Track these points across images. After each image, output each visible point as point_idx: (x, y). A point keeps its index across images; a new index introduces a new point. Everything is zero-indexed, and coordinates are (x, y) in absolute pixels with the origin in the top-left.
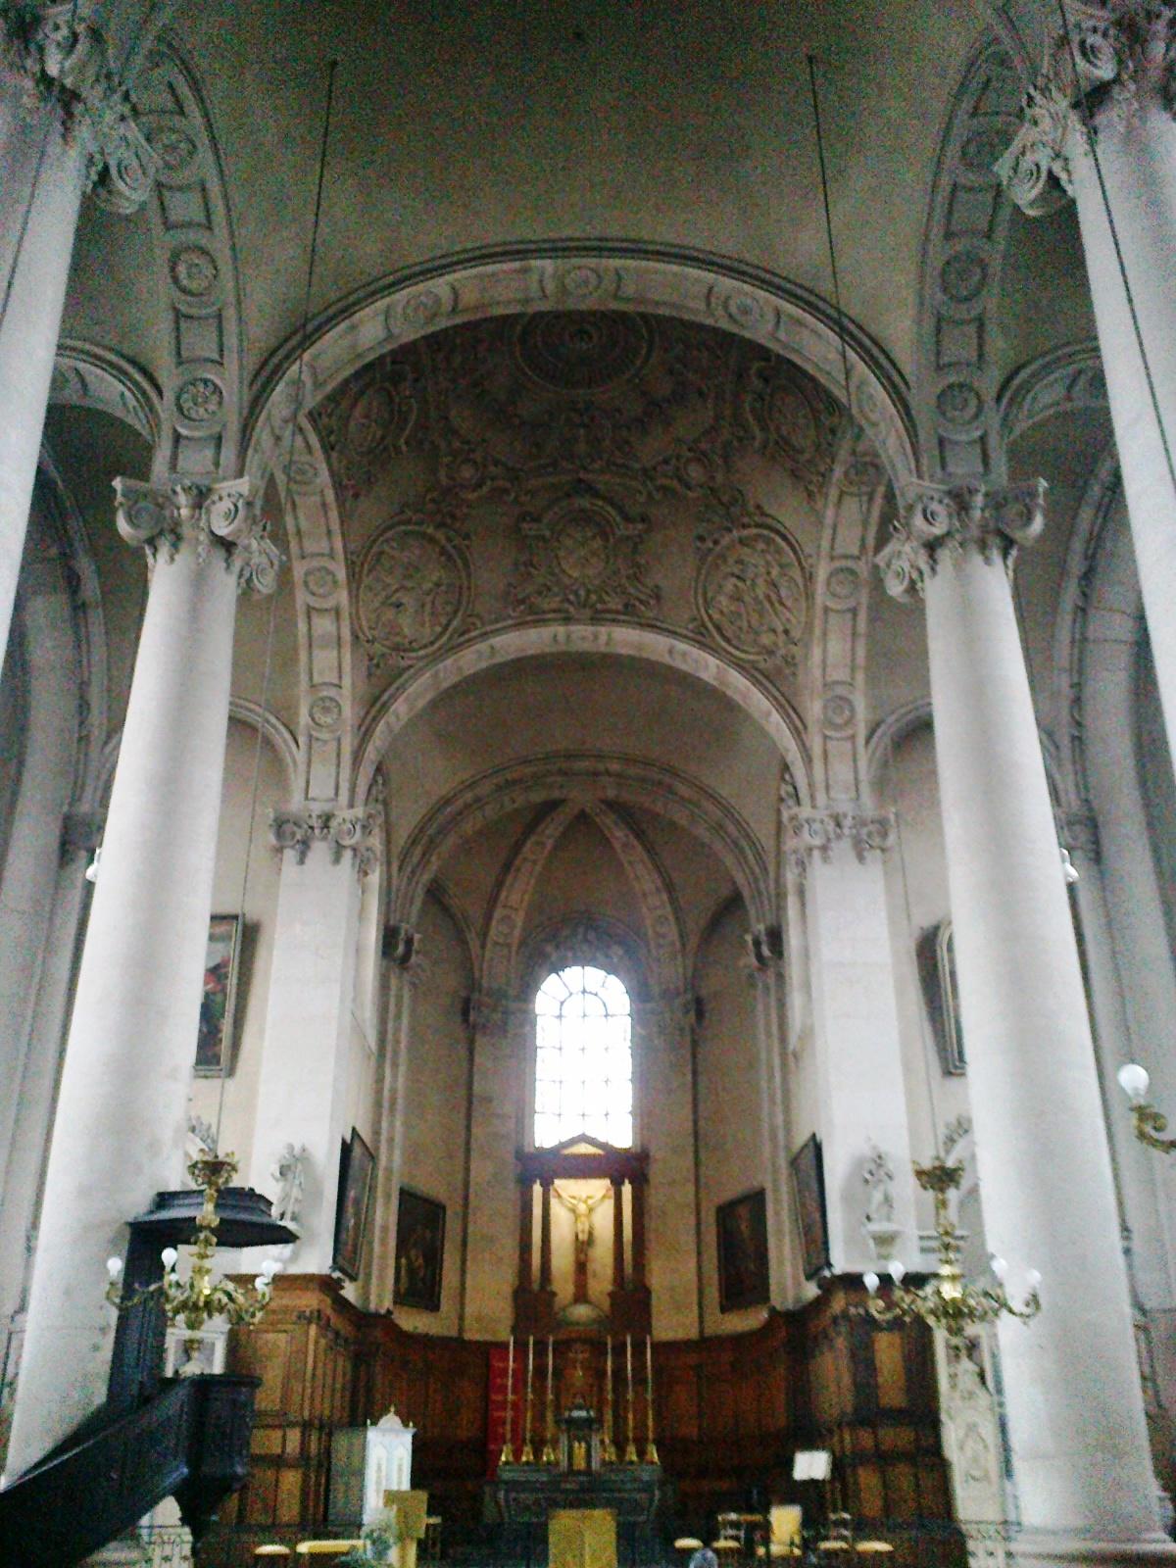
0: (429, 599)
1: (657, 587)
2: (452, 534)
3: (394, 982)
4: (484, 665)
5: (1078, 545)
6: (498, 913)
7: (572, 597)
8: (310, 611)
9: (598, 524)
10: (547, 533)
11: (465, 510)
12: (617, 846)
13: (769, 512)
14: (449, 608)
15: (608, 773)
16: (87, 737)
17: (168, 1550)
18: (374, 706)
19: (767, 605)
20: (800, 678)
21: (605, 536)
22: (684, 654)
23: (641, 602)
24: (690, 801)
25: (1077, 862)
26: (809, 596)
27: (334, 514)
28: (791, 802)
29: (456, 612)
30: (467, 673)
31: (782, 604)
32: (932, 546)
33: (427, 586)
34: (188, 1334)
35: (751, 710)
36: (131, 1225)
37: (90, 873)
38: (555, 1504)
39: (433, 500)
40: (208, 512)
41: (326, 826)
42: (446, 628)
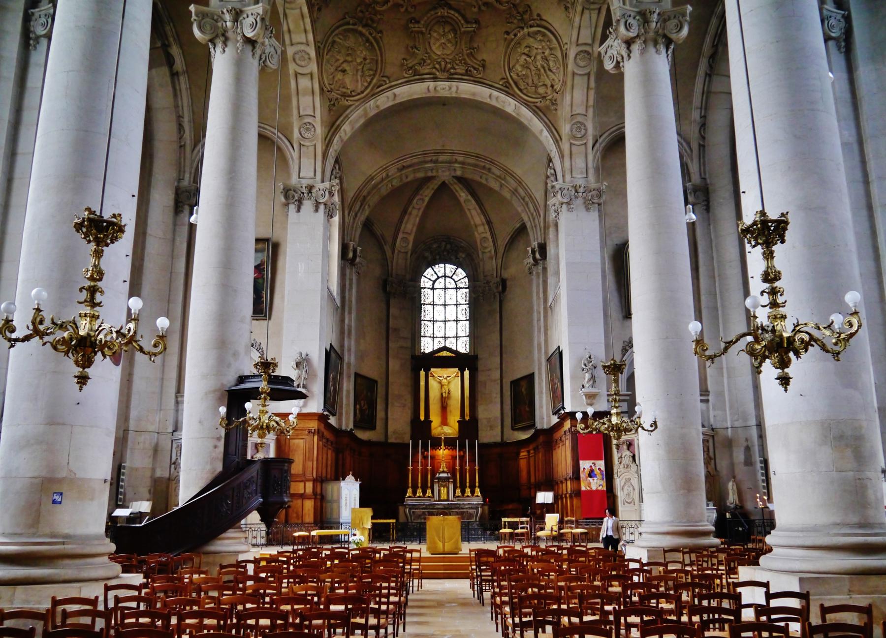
0: (360, 67)
1: (483, 60)
3: (348, 271)
4: (390, 104)
5: (708, 40)
6: (401, 236)
7: (437, 66)
8: (296, 74)
9: (451, 24)
11: (379, 17)
12: (462, 200)
13: (544, 18)
14: (371, 73)
15: (456, 161)
16: (184, 145)
17: (255, 533)
18: (332, 128)
19: (542, 70)
20: (559, 112)
21: (454, 30)
22: (497, 98)
23: (475, 69)
24: (499, 177)
25: (696, 211)
26: (565, 65)
27: (308, 20)
28: (552, 178)
29: (374, 75)
30: (382, 108)
31: (550, 70)
32: (629, 43)
33: (359, 60)
34: (259, 441)
35: (533, 129)
36: (228, 391)
37: (192, 219)
38: (431, 514)
39: (361, 11)
40: (241, 24)
41: (310, 192)
42: (369, 84)
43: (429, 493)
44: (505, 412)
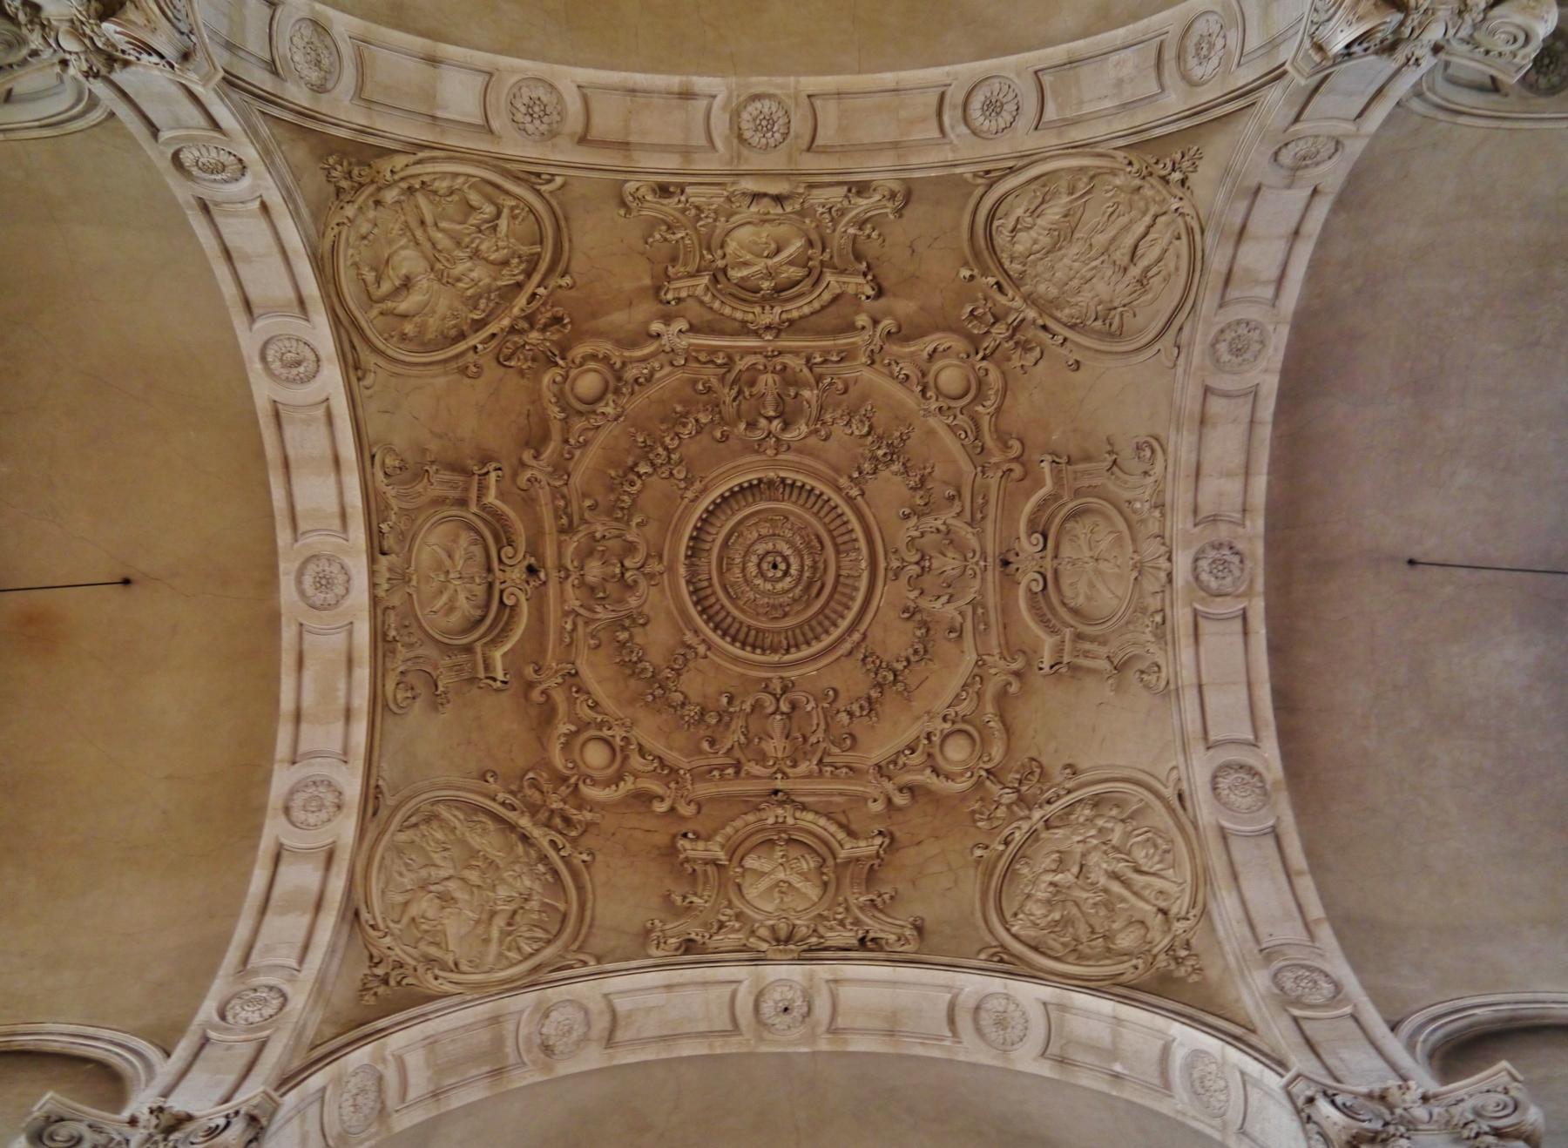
2: (560, 840)
10: (721, 855)
11: (588, 816)
14: (540, 934)
19: (1116, 887)
29: (549, 942)
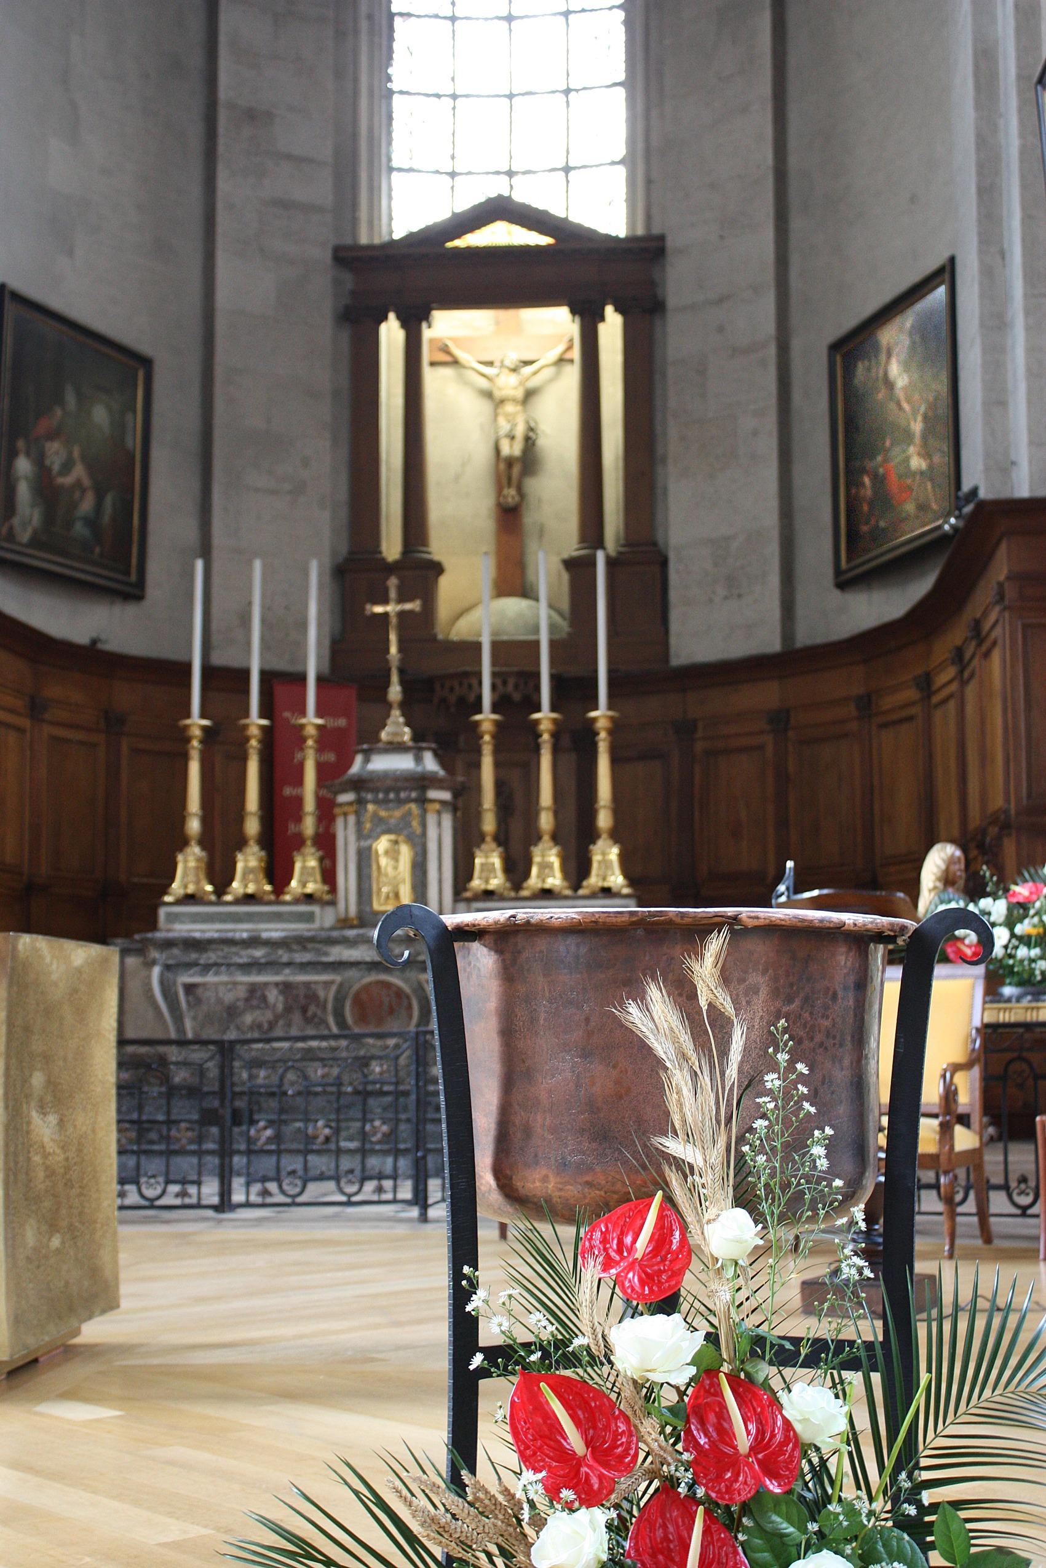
43: (305, 867)
44: (801, 500)
